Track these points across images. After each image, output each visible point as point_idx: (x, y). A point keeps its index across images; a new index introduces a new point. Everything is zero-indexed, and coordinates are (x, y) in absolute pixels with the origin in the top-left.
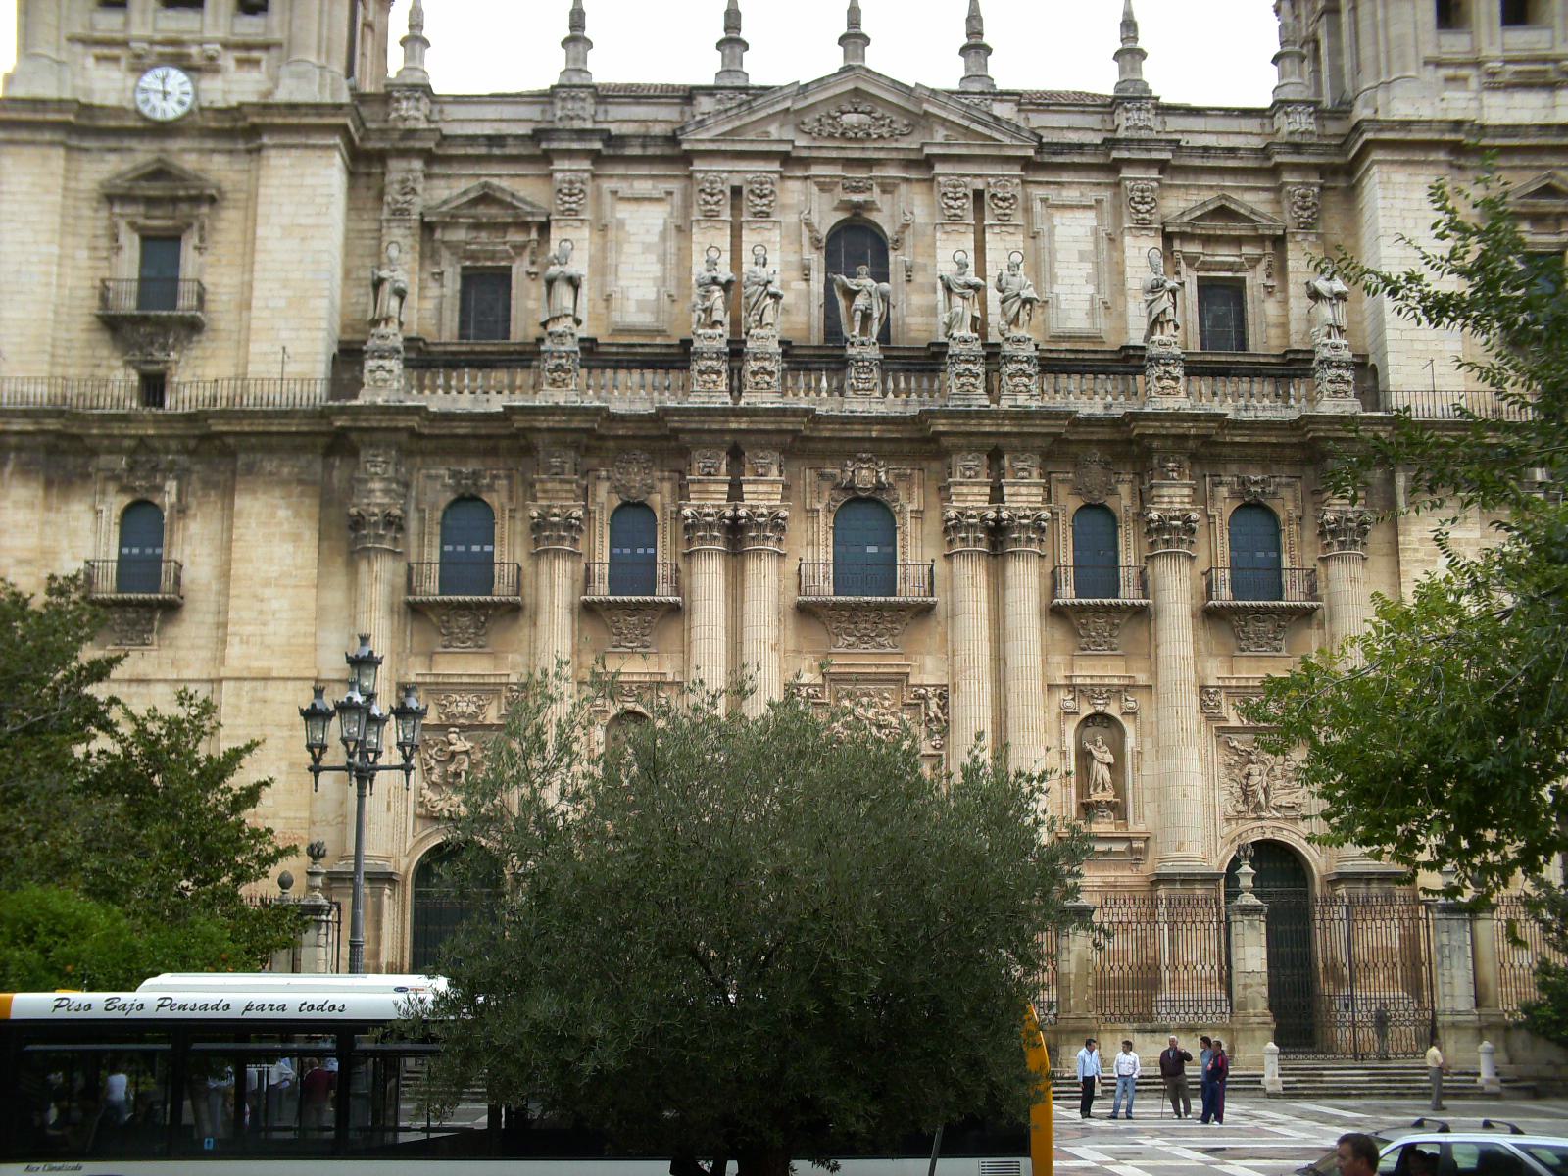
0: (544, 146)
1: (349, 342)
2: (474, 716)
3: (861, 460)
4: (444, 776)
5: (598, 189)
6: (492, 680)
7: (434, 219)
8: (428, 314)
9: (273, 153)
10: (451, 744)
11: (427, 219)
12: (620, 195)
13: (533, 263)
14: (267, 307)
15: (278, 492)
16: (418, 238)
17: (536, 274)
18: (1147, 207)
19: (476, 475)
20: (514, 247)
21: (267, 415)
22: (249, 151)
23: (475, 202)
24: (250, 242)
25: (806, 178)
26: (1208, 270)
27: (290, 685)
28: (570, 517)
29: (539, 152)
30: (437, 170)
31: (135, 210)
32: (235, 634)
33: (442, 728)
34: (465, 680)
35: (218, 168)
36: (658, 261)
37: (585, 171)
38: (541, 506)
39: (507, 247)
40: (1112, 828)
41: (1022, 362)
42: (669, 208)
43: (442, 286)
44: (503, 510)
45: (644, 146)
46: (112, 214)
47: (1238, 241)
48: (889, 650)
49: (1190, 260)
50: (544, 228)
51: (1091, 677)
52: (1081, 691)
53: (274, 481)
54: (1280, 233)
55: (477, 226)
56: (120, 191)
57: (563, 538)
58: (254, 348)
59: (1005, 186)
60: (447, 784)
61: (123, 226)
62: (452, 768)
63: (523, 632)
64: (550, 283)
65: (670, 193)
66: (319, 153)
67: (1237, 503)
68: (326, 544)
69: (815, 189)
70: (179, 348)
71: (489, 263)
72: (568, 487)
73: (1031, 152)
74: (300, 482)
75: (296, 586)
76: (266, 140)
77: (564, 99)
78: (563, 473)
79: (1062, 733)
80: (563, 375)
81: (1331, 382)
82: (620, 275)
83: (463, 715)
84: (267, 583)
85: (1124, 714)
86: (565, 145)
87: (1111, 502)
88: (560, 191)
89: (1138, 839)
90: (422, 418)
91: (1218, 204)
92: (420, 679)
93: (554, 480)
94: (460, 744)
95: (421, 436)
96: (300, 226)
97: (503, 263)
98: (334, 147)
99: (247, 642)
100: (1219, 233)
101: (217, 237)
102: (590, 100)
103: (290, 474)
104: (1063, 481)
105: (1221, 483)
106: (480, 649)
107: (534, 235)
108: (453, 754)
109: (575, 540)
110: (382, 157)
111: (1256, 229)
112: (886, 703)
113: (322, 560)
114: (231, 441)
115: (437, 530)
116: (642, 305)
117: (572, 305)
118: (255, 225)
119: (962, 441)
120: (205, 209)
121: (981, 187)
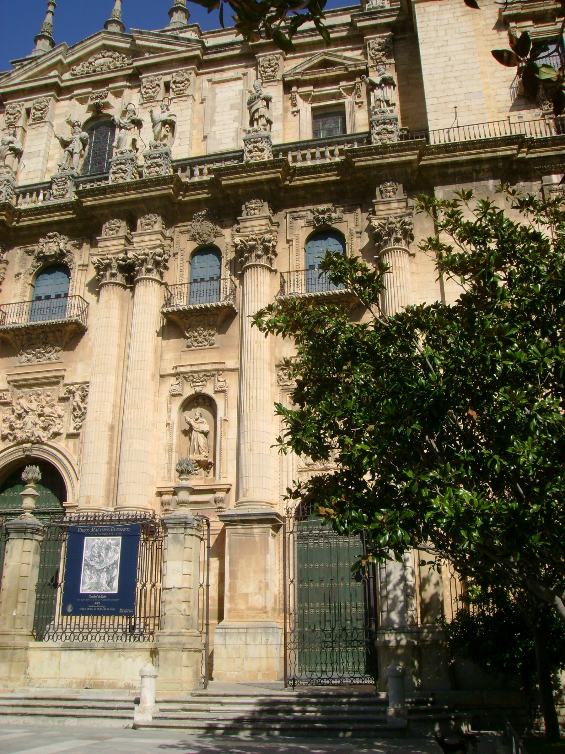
3: (50, 237)
18: (273, 69)
25: (70, 99)
26: (319, 101)
40: (201, 483)
41: (155, 158)
47: (335, 80)
48: (54, 361)
49: (305, 97)
51: (191, 365)
52: (185, 378)
54: (363, 67)
59: (183, 75)
67: (311, 230)
69: (77, 103)
73: (198, 52)
79: (169, 411)
81: (378, 134)
85: (216, 392)
87: (217, 242)
89: (220, 490)
91: (321, 58)
100: (321, 75)
104: (183, 232)
105: (298, 218)
111: (346, 69)
112: (48, 399)
119: (107, 211)
121: (169, 80)
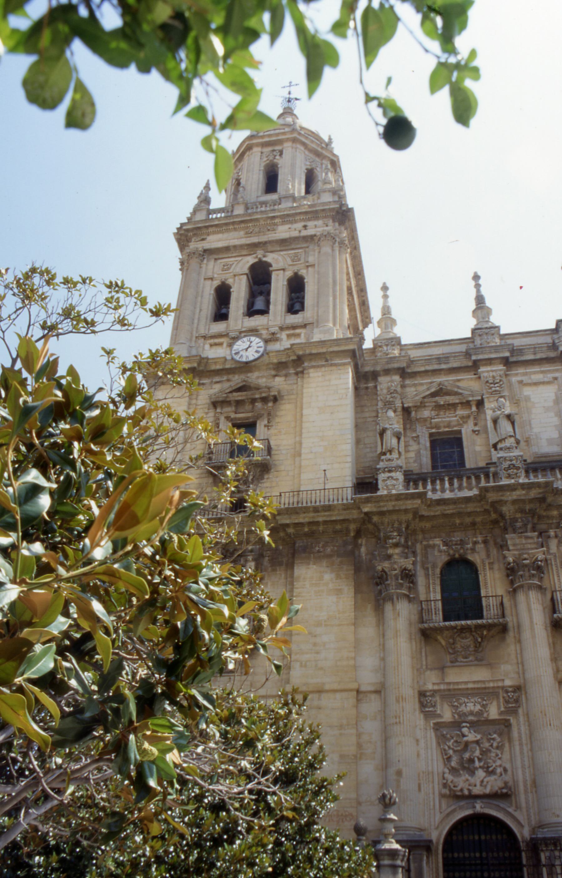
0: (474, 358)
1: (362, 478)
2: (480, 713)
4: (461, 762)
5: (510, 382)
6: (491, 685)
7: (410, 405)
8: (412, 461)
9: (311, 370)
10: (464, 736)
11: (405, 405)
12: (525, 382)
13: (476, 424)
14: (312, 452)
15: (324, 563)
16: (401, 417)
17: (478, 431)
19: (462, 543)
20: (462, 418)
21: (316, 510)
22: (297, 374)
23: (433, 395)
24: (299, 419)
27: (338, 695)
28: (537, 560)
29: (470, 364)
30: (408, 382)
31: (229, 410)
32: (297, 661)
33: (456, 725)
34: (470, 686)
35: (279, 383)
36: (556, 415)
37: (500, 370)
38: (514, 555)
39: (457, 418)
42: (556, 387)
43: (419, 443)
44: (484, 565)
45: (535, 354)
46: (216, 413)
50: (480, 404)
53: (320, 557)
55: (439, 407)
56: (221, 399)
57: (533, 575)
58: (303, 476)
60: (464, 768)
61: (222, 419)
62: (467, 755)
63: (511, 648)
64: (495, 421)
65: (556, 379)
66: (340, 367)
68: (359, 596)
70: (255, 482)
71: (447, 429)
72: (530, 541)
74: (339, 556)
75: (339, 625)
76: (306, 364)
77: (480, 335)
78: (526, 532)
80: (515, 471)
82: (533, 426)
83: (471, 713)
84: (319, 624)
86: (486, 356)
88: (487, 382)
90: (422, 502)
92: (436, 687)
93: (521, 537)
94: (471, 736)
95: (422, 517)
96: (329, 406)
97: (455, 429)
98: (348, 364)
99: (306, 666)
101: (277, 420)
102: (496, 336)
103: (332, 551)
106: (480, 662)
107: (474, 408)
108: (467, 744)
109: (541, 579)
110: (375, 375)
113: (356, 608)
114: (291, 530)
115: (438, 582)
116: (550, 442)
117: (511, 430)
118: (302, 408)
120: (270, 404)
